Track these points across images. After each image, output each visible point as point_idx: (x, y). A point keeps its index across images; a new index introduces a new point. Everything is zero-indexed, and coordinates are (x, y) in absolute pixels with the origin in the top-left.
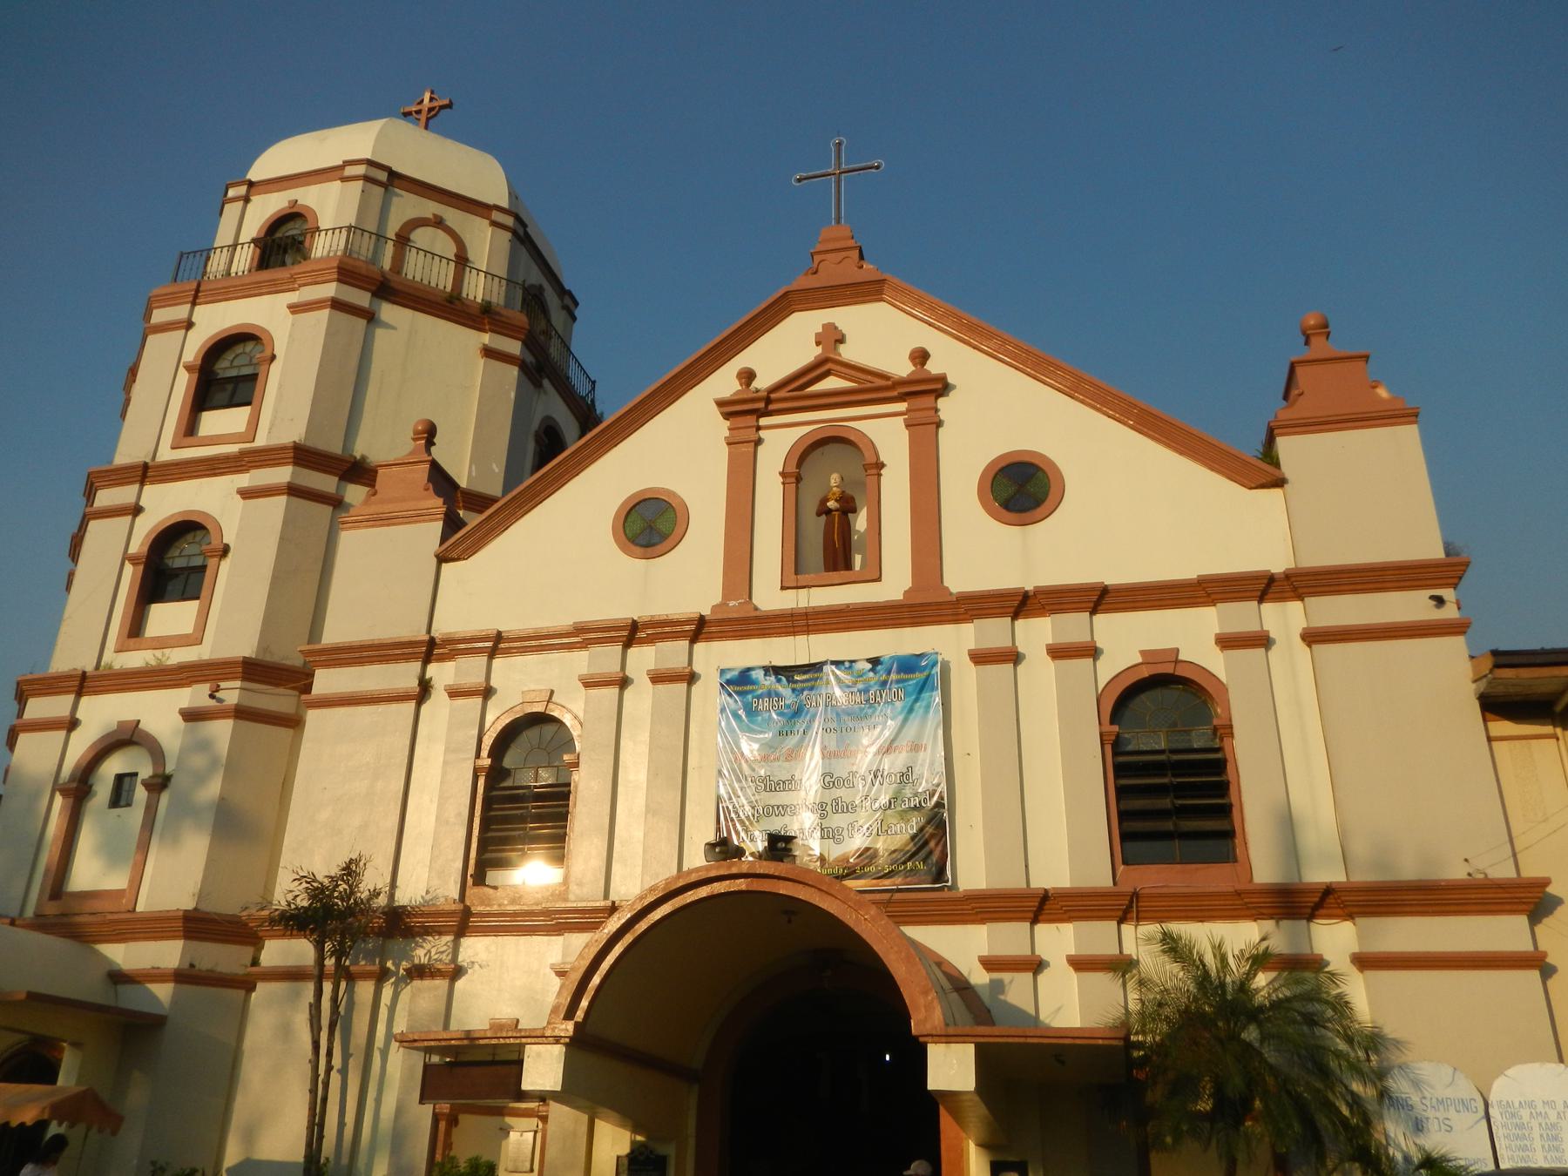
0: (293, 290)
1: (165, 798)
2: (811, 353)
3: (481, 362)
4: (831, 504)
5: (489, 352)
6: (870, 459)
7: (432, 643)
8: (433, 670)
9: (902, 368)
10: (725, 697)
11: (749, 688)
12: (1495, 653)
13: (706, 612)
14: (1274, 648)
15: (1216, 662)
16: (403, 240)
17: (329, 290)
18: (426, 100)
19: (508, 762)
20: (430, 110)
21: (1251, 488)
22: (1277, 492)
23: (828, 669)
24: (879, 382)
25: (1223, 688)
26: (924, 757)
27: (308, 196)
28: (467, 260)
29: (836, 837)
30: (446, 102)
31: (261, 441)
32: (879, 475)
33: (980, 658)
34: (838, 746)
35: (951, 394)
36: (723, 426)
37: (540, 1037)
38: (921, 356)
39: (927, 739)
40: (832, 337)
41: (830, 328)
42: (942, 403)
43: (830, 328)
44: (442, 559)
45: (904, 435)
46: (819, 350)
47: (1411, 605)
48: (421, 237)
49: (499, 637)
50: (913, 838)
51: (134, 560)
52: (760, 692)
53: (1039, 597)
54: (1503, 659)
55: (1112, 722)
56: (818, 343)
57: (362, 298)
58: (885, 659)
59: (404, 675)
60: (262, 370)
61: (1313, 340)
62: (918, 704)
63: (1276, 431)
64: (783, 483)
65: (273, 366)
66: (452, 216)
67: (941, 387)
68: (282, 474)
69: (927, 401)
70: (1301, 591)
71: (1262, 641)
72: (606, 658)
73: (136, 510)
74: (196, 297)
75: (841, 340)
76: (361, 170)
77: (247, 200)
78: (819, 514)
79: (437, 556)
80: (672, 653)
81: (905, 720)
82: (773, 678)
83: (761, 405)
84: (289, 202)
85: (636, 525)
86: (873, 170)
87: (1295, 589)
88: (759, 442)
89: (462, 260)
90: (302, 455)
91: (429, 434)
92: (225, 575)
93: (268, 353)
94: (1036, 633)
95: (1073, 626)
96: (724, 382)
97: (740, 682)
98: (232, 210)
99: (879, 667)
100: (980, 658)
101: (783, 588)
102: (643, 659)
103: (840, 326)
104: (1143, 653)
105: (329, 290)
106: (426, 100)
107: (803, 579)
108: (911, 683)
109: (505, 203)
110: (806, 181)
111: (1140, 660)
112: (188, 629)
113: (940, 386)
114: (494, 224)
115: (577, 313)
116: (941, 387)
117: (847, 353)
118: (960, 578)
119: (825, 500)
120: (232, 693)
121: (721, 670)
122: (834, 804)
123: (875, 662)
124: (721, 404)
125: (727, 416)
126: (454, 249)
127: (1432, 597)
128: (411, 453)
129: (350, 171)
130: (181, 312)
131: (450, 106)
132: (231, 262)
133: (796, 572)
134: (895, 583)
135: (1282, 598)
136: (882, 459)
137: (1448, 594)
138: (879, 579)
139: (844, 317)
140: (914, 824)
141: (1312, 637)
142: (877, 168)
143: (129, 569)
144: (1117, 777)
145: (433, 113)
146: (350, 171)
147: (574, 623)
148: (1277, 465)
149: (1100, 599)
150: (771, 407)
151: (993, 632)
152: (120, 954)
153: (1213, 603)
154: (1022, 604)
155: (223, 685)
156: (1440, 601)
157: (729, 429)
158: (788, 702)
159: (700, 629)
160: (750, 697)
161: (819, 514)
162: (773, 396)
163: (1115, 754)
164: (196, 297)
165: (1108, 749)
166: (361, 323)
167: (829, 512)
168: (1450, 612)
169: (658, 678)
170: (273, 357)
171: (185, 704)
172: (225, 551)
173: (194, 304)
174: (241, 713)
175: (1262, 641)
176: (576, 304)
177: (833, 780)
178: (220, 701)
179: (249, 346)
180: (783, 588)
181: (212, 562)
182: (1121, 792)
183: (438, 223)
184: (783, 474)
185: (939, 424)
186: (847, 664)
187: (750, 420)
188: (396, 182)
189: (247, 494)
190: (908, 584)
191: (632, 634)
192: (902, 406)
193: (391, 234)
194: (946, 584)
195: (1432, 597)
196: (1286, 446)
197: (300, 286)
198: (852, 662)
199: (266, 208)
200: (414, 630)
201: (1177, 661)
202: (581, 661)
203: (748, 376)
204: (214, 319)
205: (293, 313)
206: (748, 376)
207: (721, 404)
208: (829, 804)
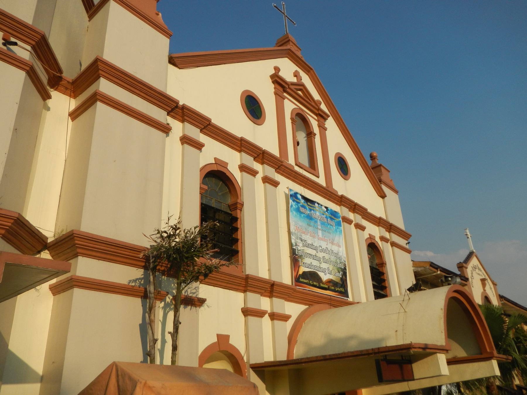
10: (291, 201)
11: (298, 201)
12: (432, 263)
21: (378, 196)
22: (381, 199)
23: (316, 204)
26: (341, 249)
29: (325, 272)
34: (322, 236)
36: (273, 86)
39: (341, 244)
47: (402, 242)
50: (342, 279)
52: (301, 204)
53: (357, 206)
54: (432, 265)
58: (329, 209)
62: (338, 230)
64: (292, 123)
69: (321, 120)
70: (392, 230)
81: (336, 235)
82: (303, 200)
87: (390, 229)
97: (294, 196)
99: (328, 211)
104: (369, 234)
108: (336, 221)
121: (290, 189)
122: (323, 259)
123: (326, 208)
125: (273, 82)
134: (321, 181)
140: (341, 274)
142: (295, 24)
147: (242, 137)
153: (378, 226)
158: (308, 213)
160: (299, 205)
168: (407, 247)
177: (322, 249)
186: (320, 205)
192: (316, 118)
194: (334, 188)
198: (321, 205)
203: (277, 69)
208: (322, 259)
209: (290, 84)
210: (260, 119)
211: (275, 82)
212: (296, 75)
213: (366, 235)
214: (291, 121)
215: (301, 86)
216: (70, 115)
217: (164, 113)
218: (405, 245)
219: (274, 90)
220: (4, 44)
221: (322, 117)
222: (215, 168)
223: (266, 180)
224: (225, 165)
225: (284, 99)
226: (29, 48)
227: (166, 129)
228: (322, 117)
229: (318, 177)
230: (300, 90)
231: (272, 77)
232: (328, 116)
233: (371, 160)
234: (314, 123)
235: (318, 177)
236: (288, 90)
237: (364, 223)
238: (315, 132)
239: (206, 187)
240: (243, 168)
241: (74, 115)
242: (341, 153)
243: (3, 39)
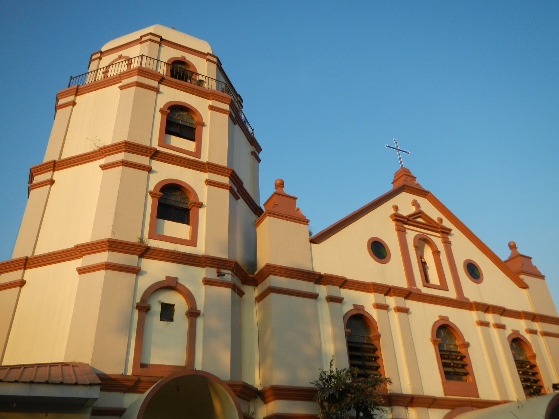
1: (200, 322)
24: (434, 225)
27: (191, 58)
32: (440, 255)
36: (393, 223)
40: (415, 203)
51: (151, 193)
60: (198, 128)
64: (416, 250)
65: (204, 128)
69: (445, 235)
83: (406, 220)
86: (407, 153)
94: (490, 318)
102: (391, 301)
103: (418, 202)
110: (389, 148)
120: (228, 277)
125: (393, 220)
134: (452, 294)
142: (408, 153)
149: (503, 312)
150: (409, 222)
155: (223, 271)
157: (396, 225)
162: (410, 218)
170: (203, 125)
172: (201, 205)
179: (185, 114)
192: (439, 235)
206: (396, 208)
209: (408, 217)
210: (386, 256)
211: (396, 220)
212: (415, 203)
213: (508, 332)
214: (414, 249)
215: (419, 214)
216: (256, 299)
217: (312, 284)
219: (395, 227)
220: (218, 276)
221: (446, 232)
222: (355, 312)
223: (399, 310)
224: (361, 308)
225: (405, 232)
226: (230, 272)
227: (314, 296)
228: (446, 232)
229: (448, 290)
230: (420, 217)
231: (391, 217)
232: (450, 230)
233: (510, 249)
234: (438, 241)
235: (448, 290)
236: (409, 222)
237: (505, 320)
238: (439, 250)
239: (349, 330)
241: (260, 298)
242: (472, 259)
243: (218, 273)
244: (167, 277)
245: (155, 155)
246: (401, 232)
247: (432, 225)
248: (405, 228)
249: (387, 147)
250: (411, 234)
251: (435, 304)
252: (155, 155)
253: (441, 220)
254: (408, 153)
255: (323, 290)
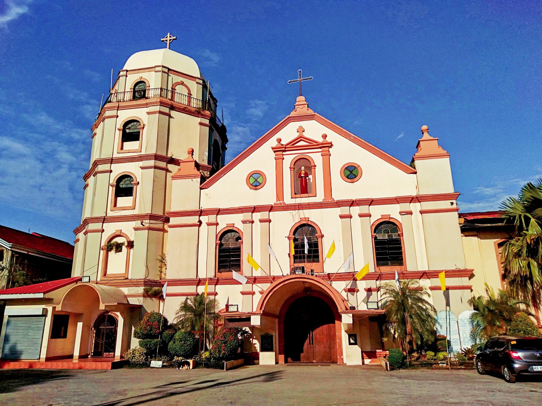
0: (147, 107)
2: (296, 135)
3: (199, 126)
4: (302, 175)
5: (201, 124)
6: (312, 164)
7: (201, 211)
8: (202, 218)
9: (320, 140)
13: (273, 204)
14: (413, 215)
15: (399, 218)
16: (173, 89)
17: (157, 108)
18: (168, 37)
19: (223, 242)
20: (170, 40)
22: (415, 175)
24: (315, 144)
25: (401, 224)
28: (191, 95)
30: (175, 38)
31: (143, 153)
32: (315, 168)
33: (342, 217)
35: (333, 147)
37: (254, 314)
38: (325, 136)
40: (301, 130)
41: (301, 127)
42: (330, 149)
43: (301, 127)
44: (201, 189)
45: (321, 157)
46: (298, 134)
47: (445, 204)
48: (179, 89)
49: (219, 210)
55: (374, 232)
56: (298, 132)
57: (166, 110)
59: (194, 219)
61: (424, 133)
63: (415, 159)
66: (186, 81)
67: (330, 145)
68: (152, 163)
71: (410, 213)
72: (247, 216)
73: (111, 171)
74: (118, 108)
75: (304, 131)
76: (160, 69)
77: (127, 76)
78: (299, 178)
79: (200, 188)
80: (264, 215)
84: (140, 77)
85: (252, 181)
87: (418, 200)
88: (283, 159)
89: (190, 94)
90: (157, 157)
91: (192, 152)
92: (138, 190)
93: (142, 126)
94: (355, 211)
95: (364, 209)
96: (272, 142)
98: (122, 79)
100: (342, 217)
101: (292, 198)
102: (257, 216)
105: (157, 108)
106: (168, 37)
107: (297, 196)
109: (199, 77)
111: (381, 217)
112: (131, 204)
113: (330, 145)
114: (197, 83)
115: (218, 104)
116: (330, 145)
117: (305, 135)
118: (337, 196)
119: (300, 174)
124: (273, 148)
125: (275, 152)
126: (187, 92)
127: (451, 203)
128: (188, 158)
129: (157, 69)
130: (114, 113)
131: (176, 39)
132: (124, 97)
133: (295, 194)
134: (320, 197)
135: (415, 202)
136: (315, 164)
137: (454, 201)
138: (316, 196)
139: (305, 124)
141: (422, 212)
142: (311, 79)
143: (111, 188)
144: (375, 245)
145: (171, 41)
146: (157, 69)
148: (415, 168)
149: (371, 202)
151: (345, 210)
152: (125, 290)
154: (352, 203)
155: (144, 221)
156: (452, 204)
159: (271, 209)
161: (299, 178)
163: (375, 240)
164: (118, 108)
165: (373, 239)
166: (168, 117)
167: (302, 177)
168: (455, 206)
169: (261, 221)
171: (134, 226)
173: (118, 110)
174: (150, 229)
175: (410, 213)
176: (217, 102)
178: (143, 225)
180: (292, 198)
181: (135, 187)
182: (377, 249)
183: (182, 83)
184: (290, 168)
185: (330, 155)
187: (281, 153)
188: (170, 72)
189: (142, 168)
190: (323, 198)
191: (254, 209)
192: (320, 150)
193: (170, 89)
195: (451, 203)
196: (417, 163)
197: (149, 106)
199: (132, 79)
200: (194, 207)
201: (390, 218)
202: (241, 217)
203: (279, 140)
204: (125, 115)
205: (148, 114)
206: (279, 140)
207: (273, 148)
218: (450, 207)
240: (244, 222)
244: (116, 230)
245: (112, 161)
246: (279, 160)
247: (313, 145)
248: (283, 155)
249: (290, 82)
250: (289, 159)
251: (299, 209)
252: (112, 161)
253: (325, 136)
254: (311, 79)
255: (204, 219)
